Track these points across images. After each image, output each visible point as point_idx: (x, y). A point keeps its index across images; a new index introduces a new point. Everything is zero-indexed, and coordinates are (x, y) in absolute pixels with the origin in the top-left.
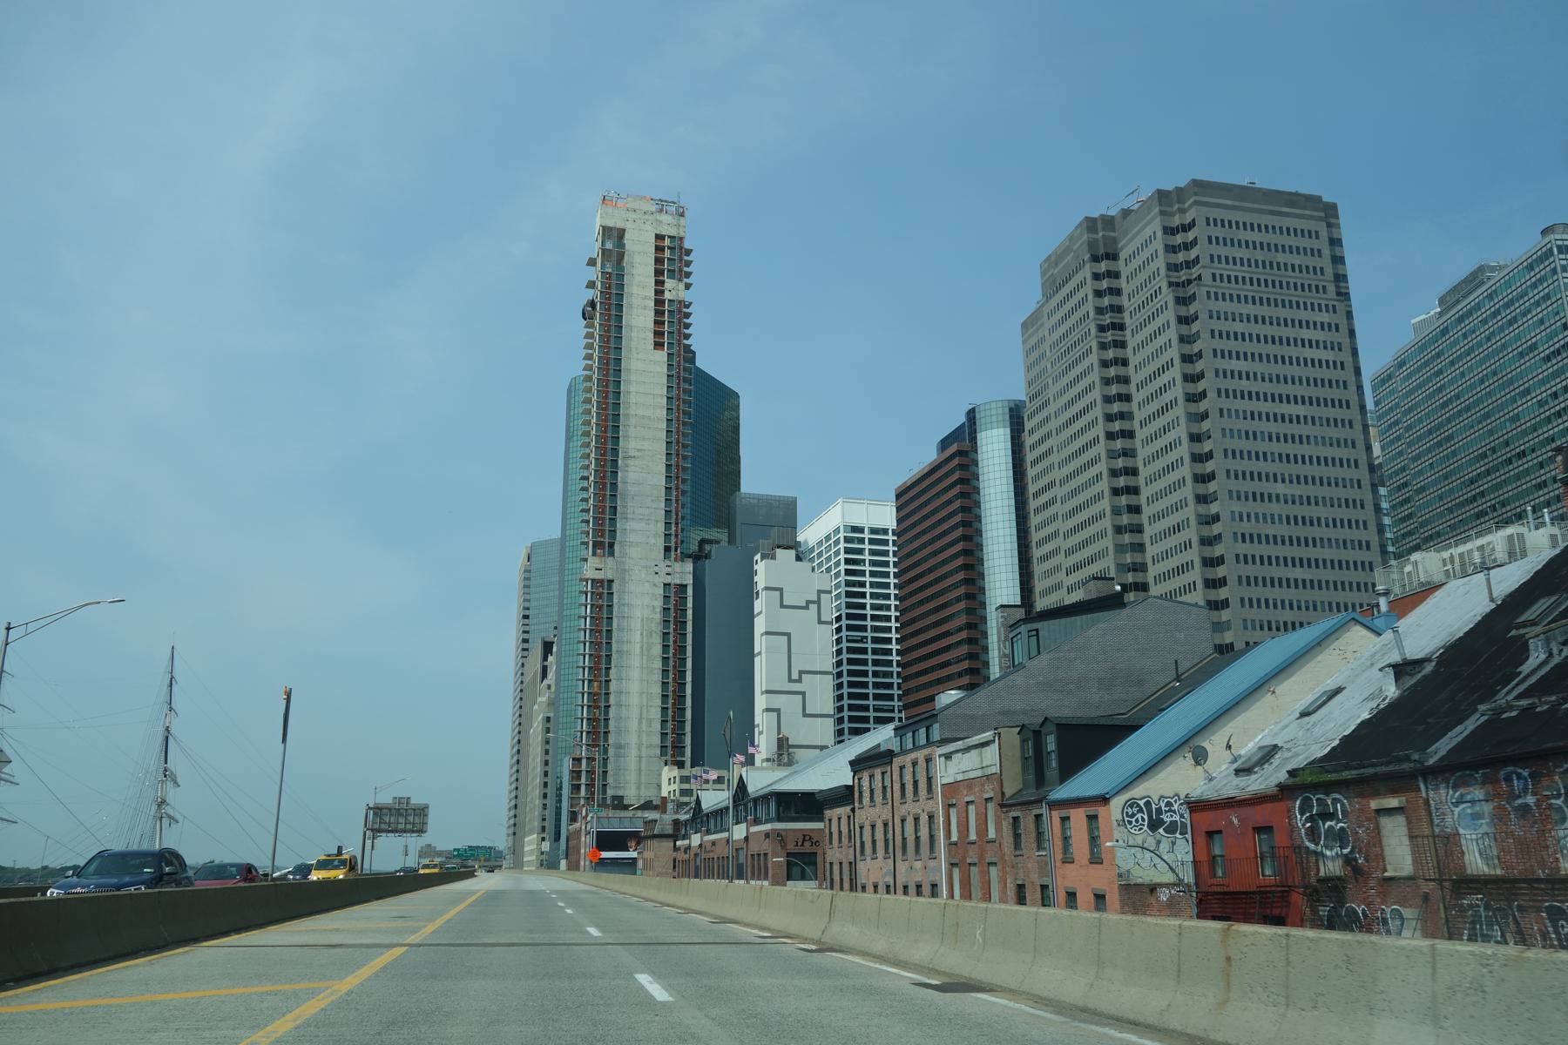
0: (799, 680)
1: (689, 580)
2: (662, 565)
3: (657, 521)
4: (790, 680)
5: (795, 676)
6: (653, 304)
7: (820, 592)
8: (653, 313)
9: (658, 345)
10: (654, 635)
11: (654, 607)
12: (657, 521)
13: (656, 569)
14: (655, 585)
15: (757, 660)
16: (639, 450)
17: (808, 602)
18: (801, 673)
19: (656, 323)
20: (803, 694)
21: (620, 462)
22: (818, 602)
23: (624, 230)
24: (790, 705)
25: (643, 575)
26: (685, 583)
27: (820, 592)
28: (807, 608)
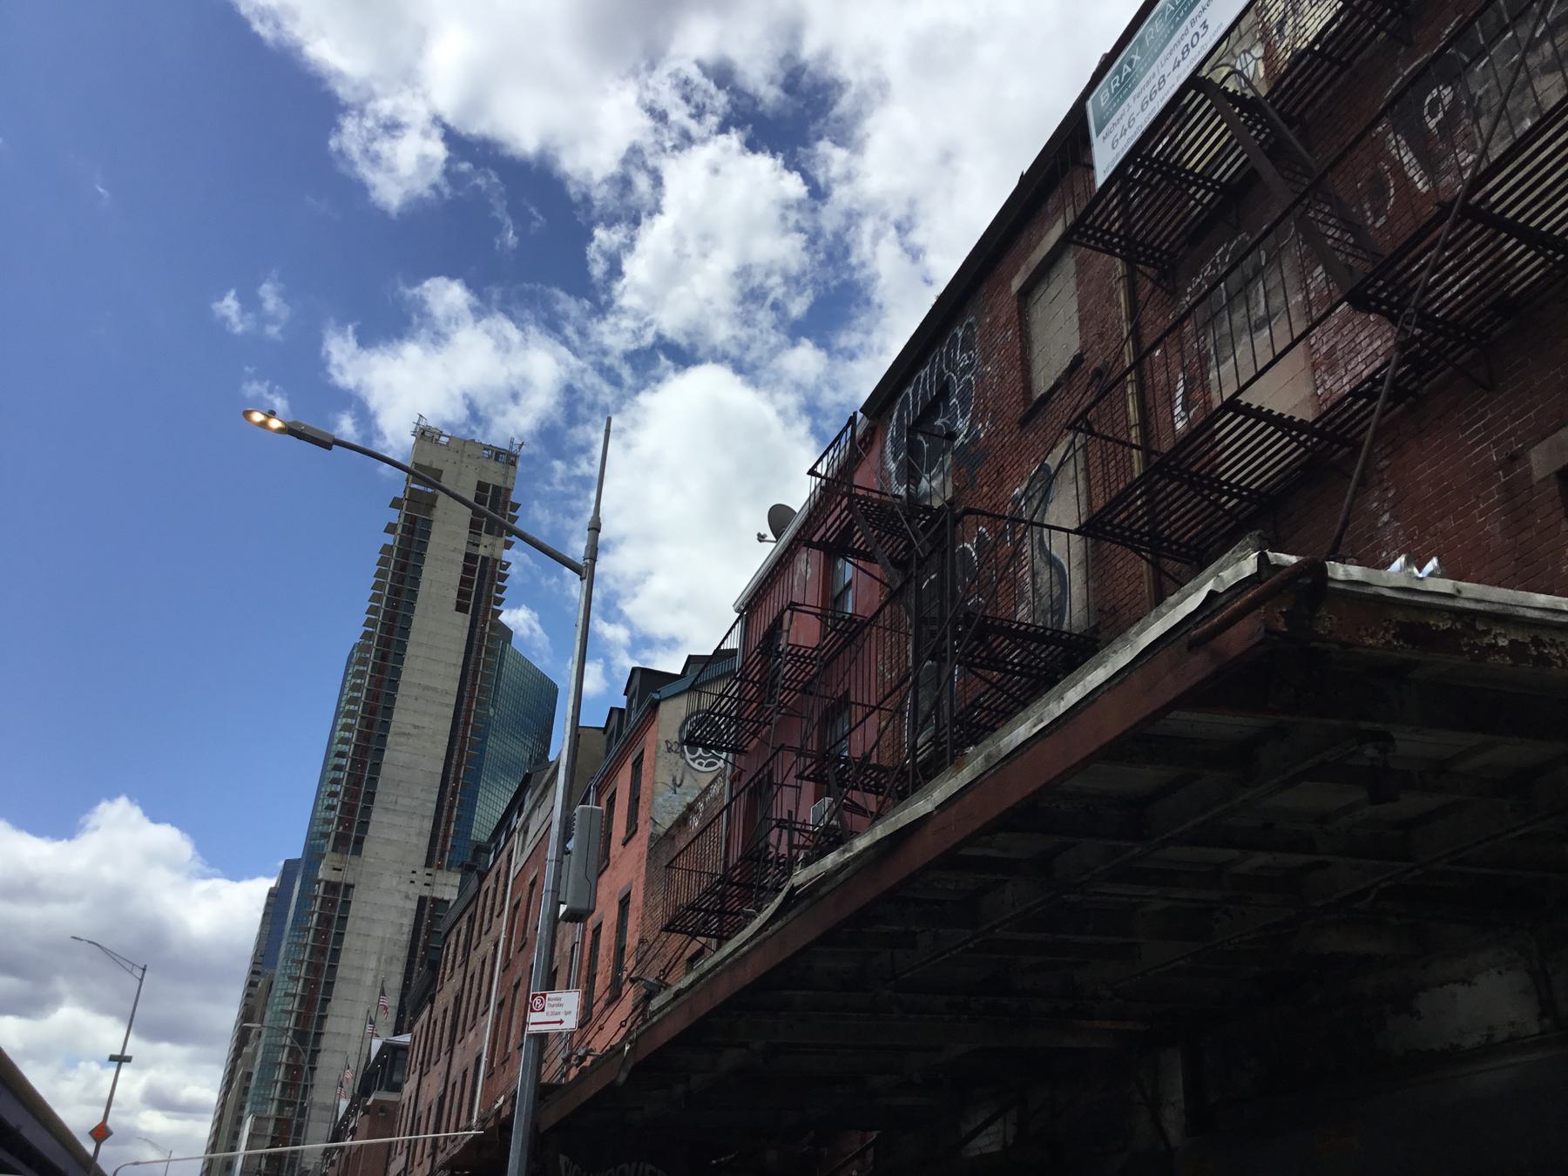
2: (421, 872)
3: (424, 817)
6: (462, 558)
8: (460, 569)
9: (461, 608)
10: (394, 961)
11: (402, 925)
12: (424, 817)
13: (414, 877)
16: (415, 727)
19: (463, 582)
23: (441, 471)
25: (394, 883)
26: (446, 898)
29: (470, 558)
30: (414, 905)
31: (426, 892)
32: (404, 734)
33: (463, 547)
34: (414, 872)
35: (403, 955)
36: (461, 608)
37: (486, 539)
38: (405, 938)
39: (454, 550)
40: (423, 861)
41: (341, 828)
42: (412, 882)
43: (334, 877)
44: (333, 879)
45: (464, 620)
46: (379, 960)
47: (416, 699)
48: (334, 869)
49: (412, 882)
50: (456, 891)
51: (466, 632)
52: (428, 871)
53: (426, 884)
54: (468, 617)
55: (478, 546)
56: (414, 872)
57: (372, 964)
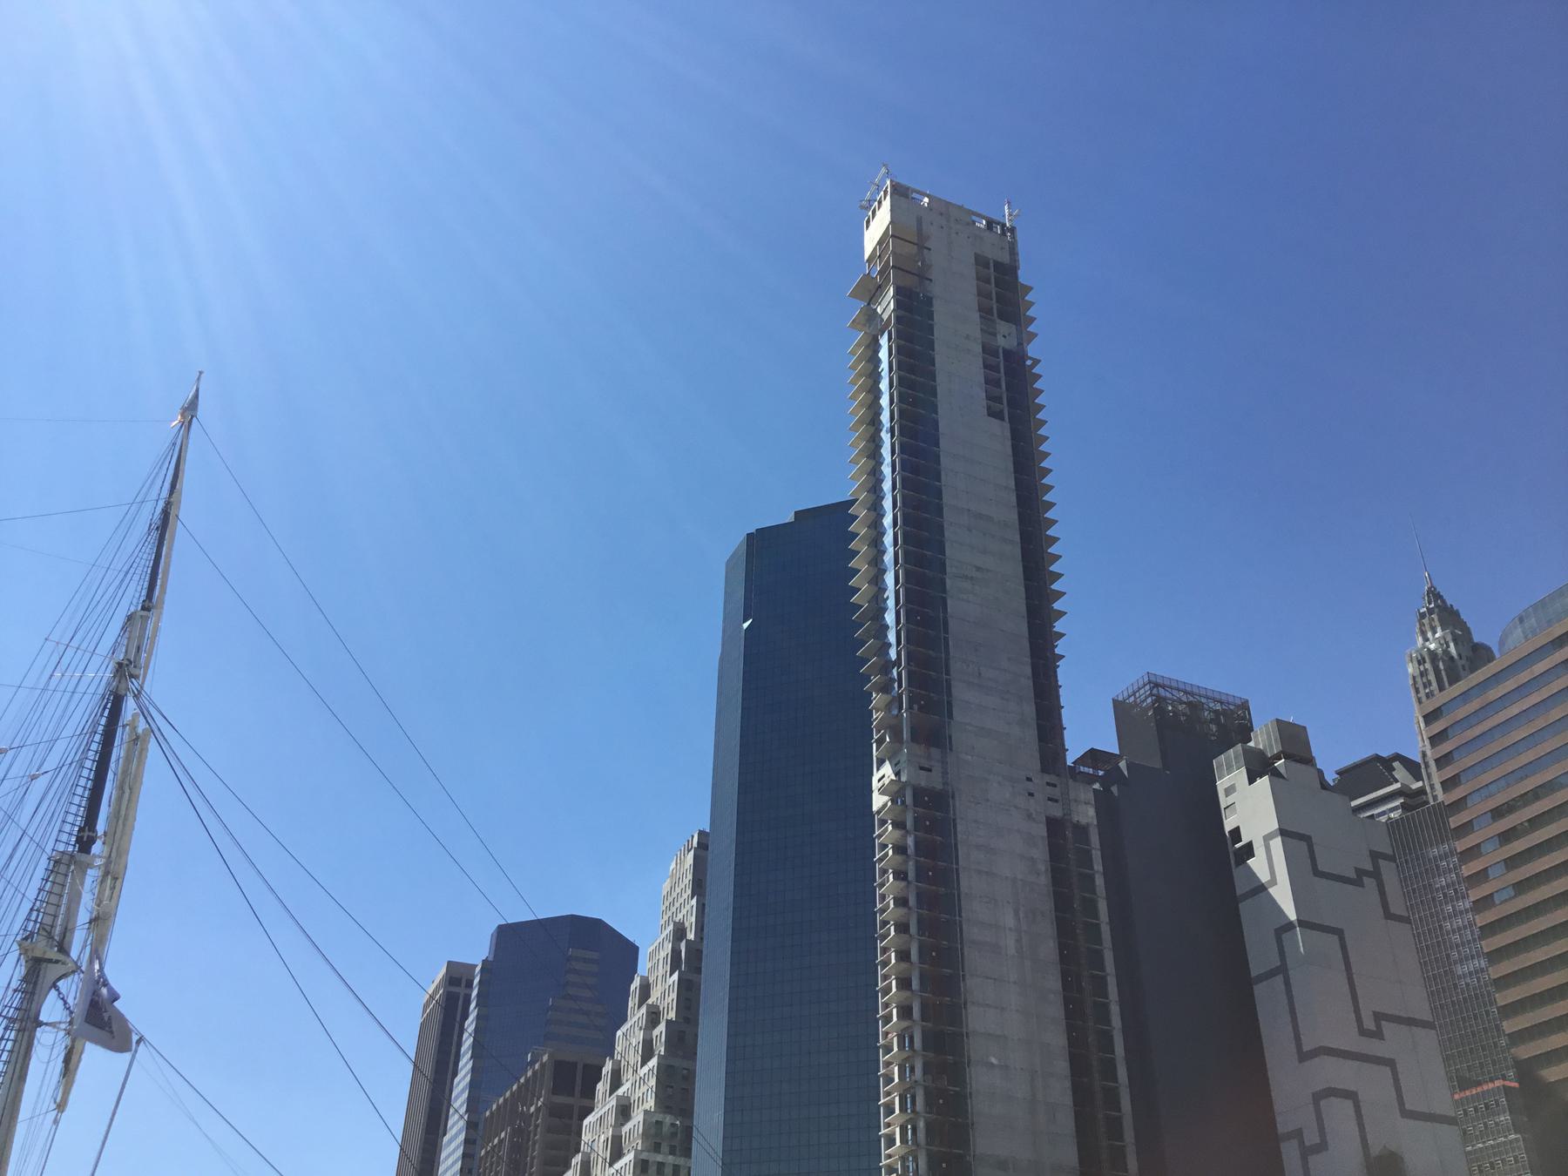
0: (1378, 1034)
1: (1087, 814)
4: (1363, 1032)
5: (1369, 1024)
7: (1375, 856)
14: (1029, 816)
15: (1259, 990)
16: (978, 569)
17: (1361, 873)
18: (1379, 1017)
20: (1390, 1063)
21: (948, 582)
22: (1376, 874)
24: (1372, 1085)
27: (1375, 856)
28: (1357, 882)
29: (988, 350)
30: (1041, 830)
31: (1056, 811)
32: (966, 577)
33: (978, 334)
34: (1029, 779)
35: (1048, 906)
36: (992, 413)
37: (1003, 327)
38: (1044, 880)
39: (967, 337)
40: (1038, 766)
41: (916, 707)
42: (1031, 795)
43: (923, 780)
44: (923, 784)
45: (1001, 429)
46: (1016, 912)
47: (970, 530)
48: (922, 768)
49: (1031, 795)
50: (1091, 812)
51: (1009, 443)
52: (1048, 778)
53: (1050, 799)
54: (1007, 425)
55: (994, 335)
56: (1029, 779)
57: (1009, 920)
